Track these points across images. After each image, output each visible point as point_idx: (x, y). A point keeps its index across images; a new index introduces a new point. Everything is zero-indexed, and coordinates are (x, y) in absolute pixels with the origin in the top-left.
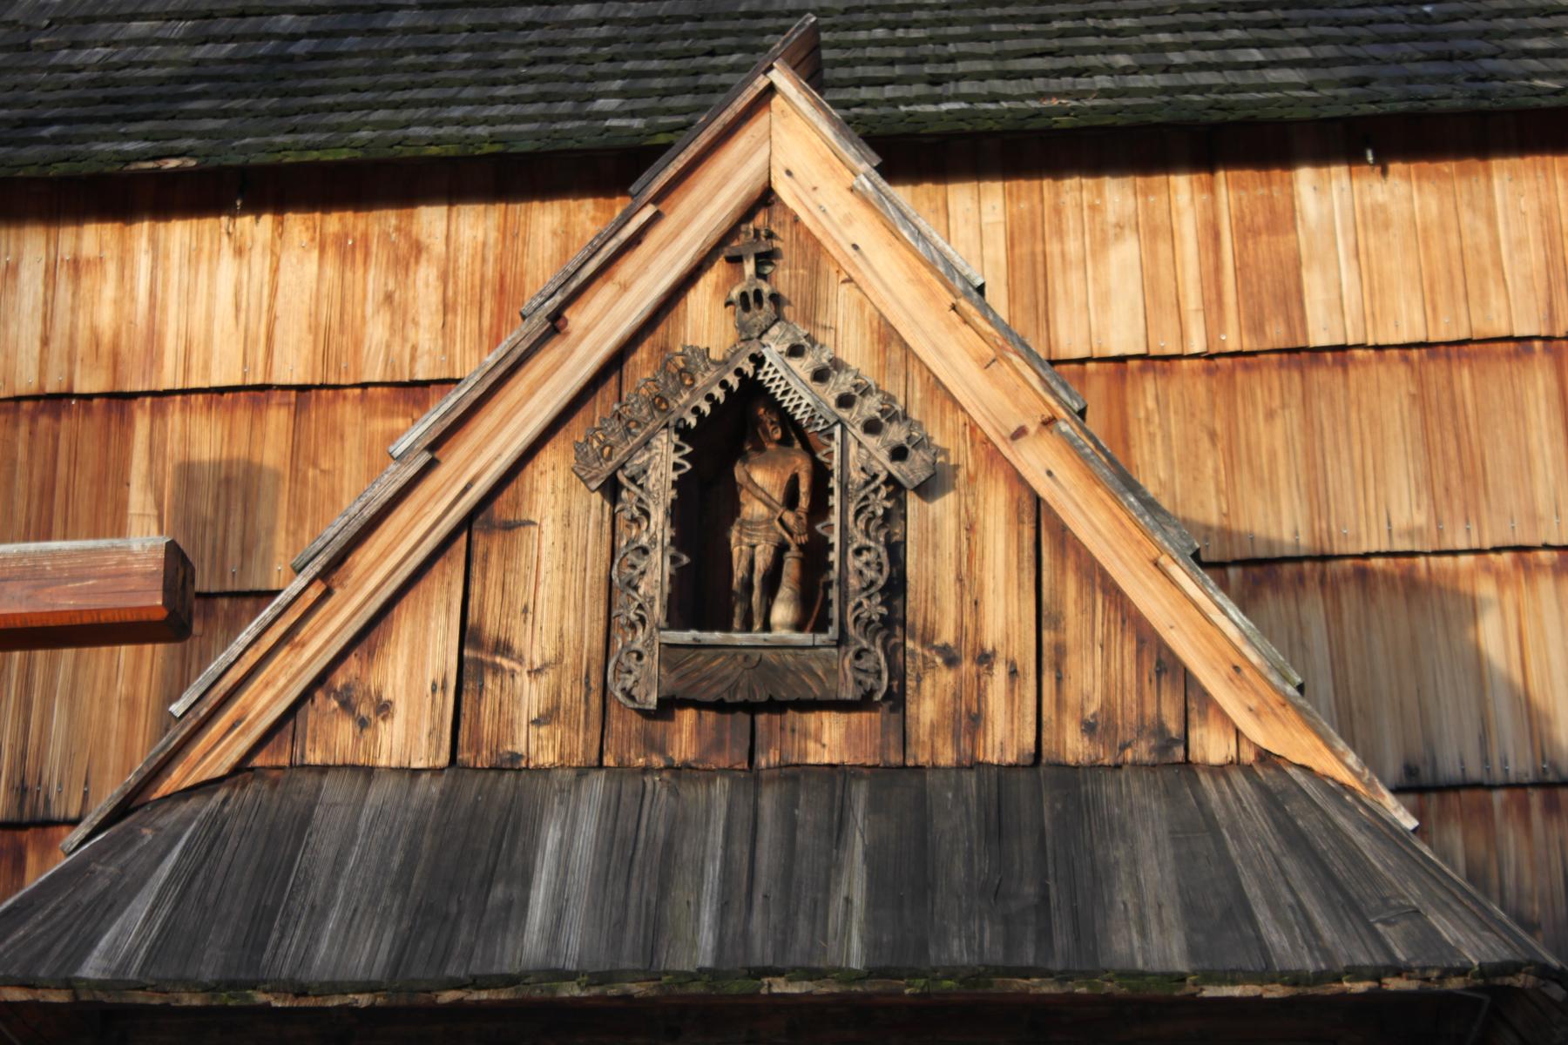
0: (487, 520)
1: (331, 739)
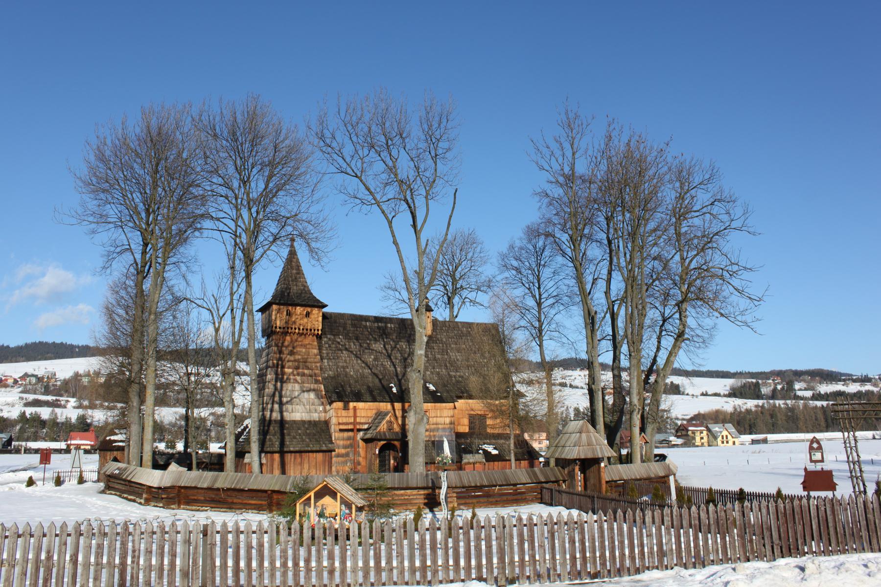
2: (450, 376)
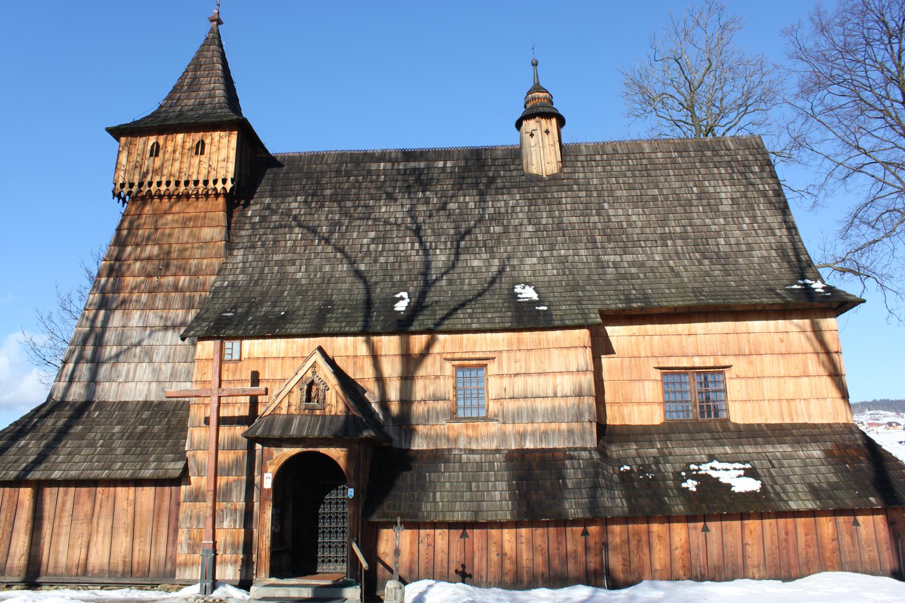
0: (290, 392)
1: (278, 411)
2: (602, 265)
